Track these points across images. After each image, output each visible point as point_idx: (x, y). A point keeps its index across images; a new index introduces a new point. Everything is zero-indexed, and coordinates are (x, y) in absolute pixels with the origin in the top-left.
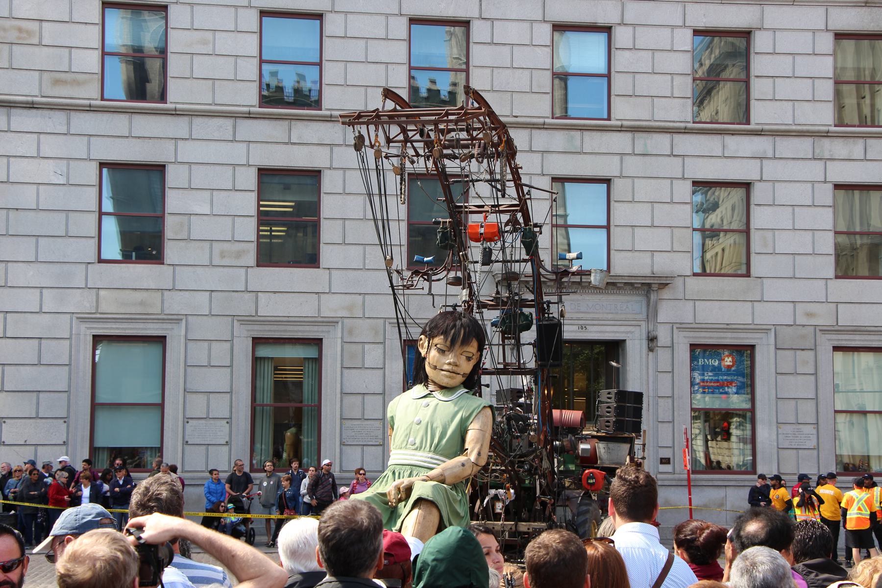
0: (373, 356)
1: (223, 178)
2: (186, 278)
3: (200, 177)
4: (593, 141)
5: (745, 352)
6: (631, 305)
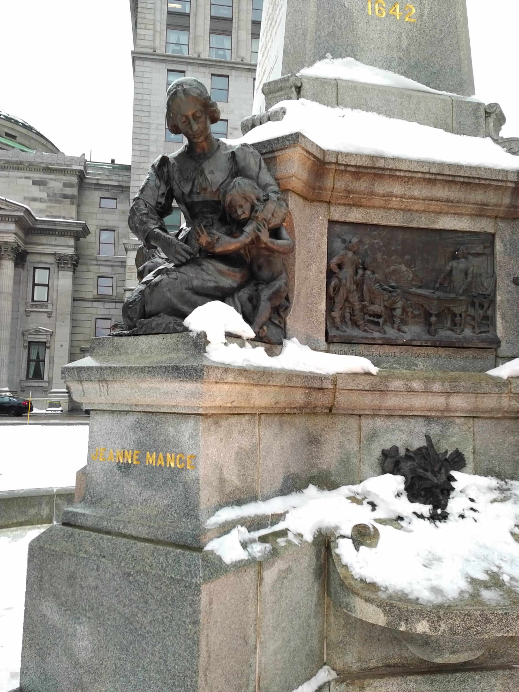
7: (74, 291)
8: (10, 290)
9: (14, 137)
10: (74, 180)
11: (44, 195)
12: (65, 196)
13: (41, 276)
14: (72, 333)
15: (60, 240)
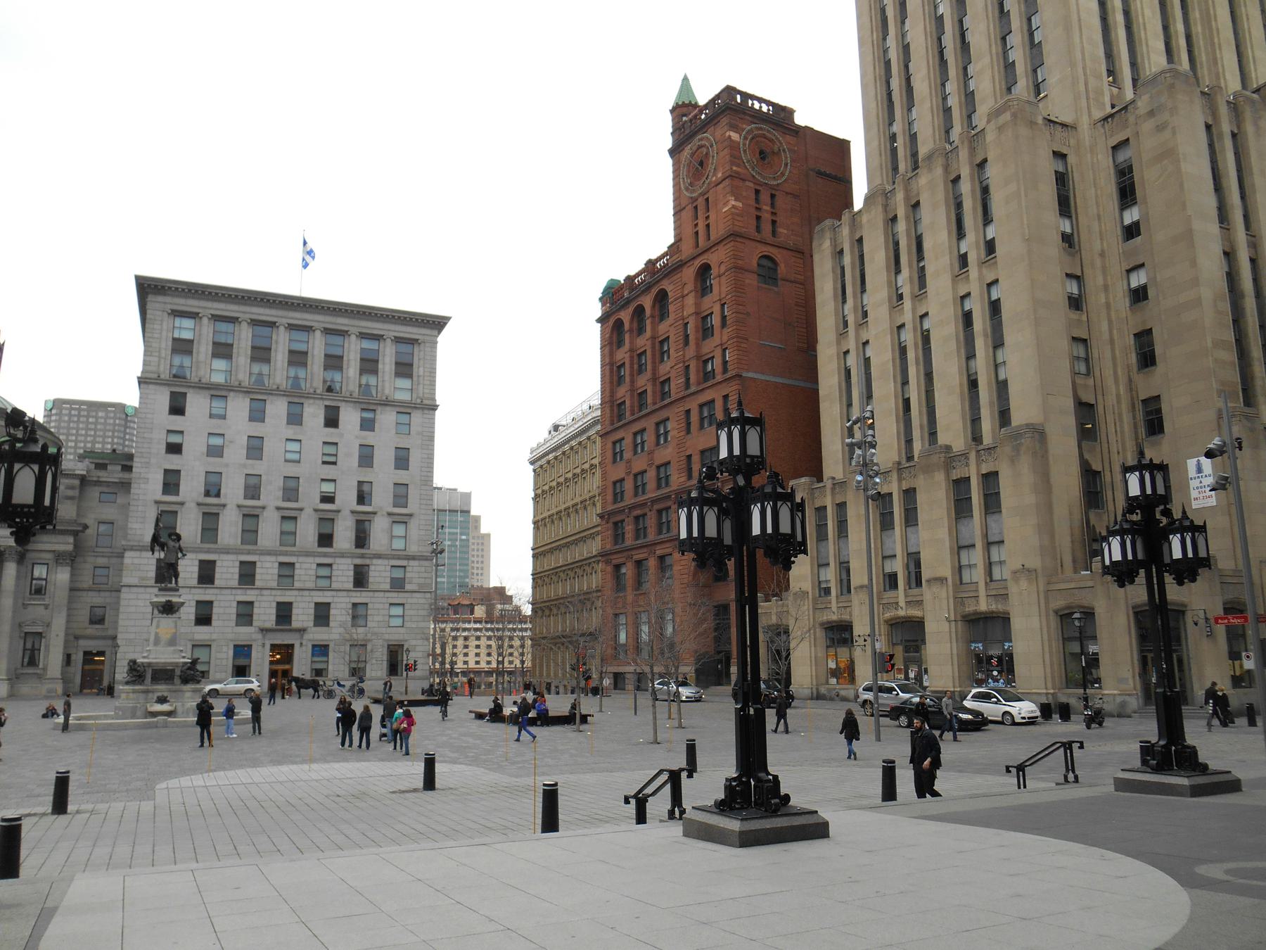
0: (225, 649)
4: (288, 593)
5: (327, 646)
6: (297, 635)
7: (71, 581)
8: (12, 589)
10: (77, 482)
13: (40, 571)
14: (68, 622)
15: (61, 538)
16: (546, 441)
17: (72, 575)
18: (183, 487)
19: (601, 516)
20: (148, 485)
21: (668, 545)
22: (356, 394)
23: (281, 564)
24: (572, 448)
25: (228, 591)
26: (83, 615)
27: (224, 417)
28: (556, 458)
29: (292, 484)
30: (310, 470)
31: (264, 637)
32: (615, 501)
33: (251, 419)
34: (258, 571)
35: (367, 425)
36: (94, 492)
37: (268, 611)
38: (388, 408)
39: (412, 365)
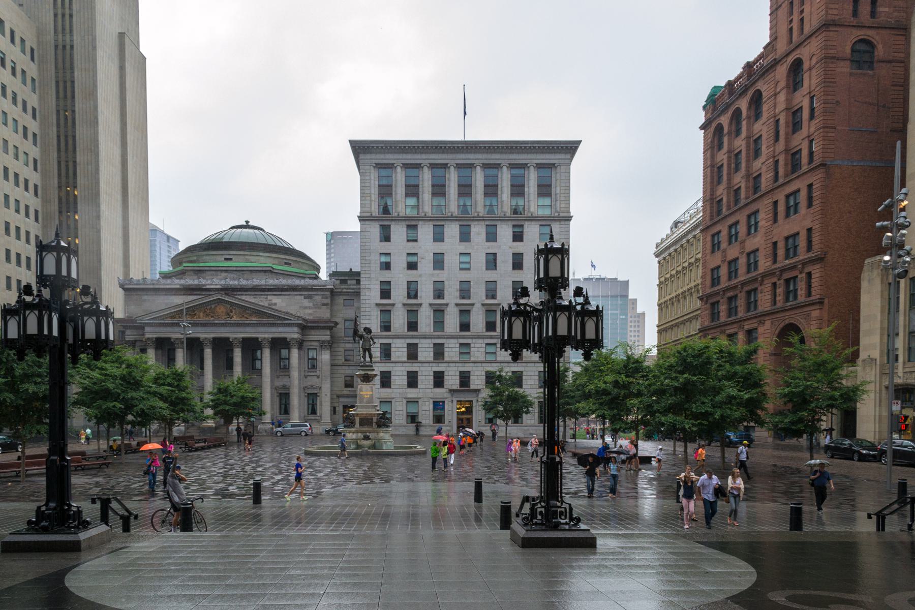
1: (401, 373)
2: (395, 391)
3: (397, 373)
4: (467, 365)
6: (475, 395)
9: (289, 264)
10: (328, 294)
11: (311, 305)
12: (324, 304)
16: (668, 236)
17: (331, 355)
18: (393, 294)
19: (701, 298)
20: (371, 294)
21: (754, 321)
22: (508, 214)
23: (461, 344)
24: (688, 241)
25: (427, 365)
26: (341, 382)
27: (416, 241)
28: (676, 250)
29: (465, 286)
30: (479, 275)
31: (452, 395)
32: (713, 285)
33: (435, 240)
34: (446, 350)
35: (518, 237)
36: (340, 300)
37: (454, 378)
38: (533, 223)
39: (550, 186)
